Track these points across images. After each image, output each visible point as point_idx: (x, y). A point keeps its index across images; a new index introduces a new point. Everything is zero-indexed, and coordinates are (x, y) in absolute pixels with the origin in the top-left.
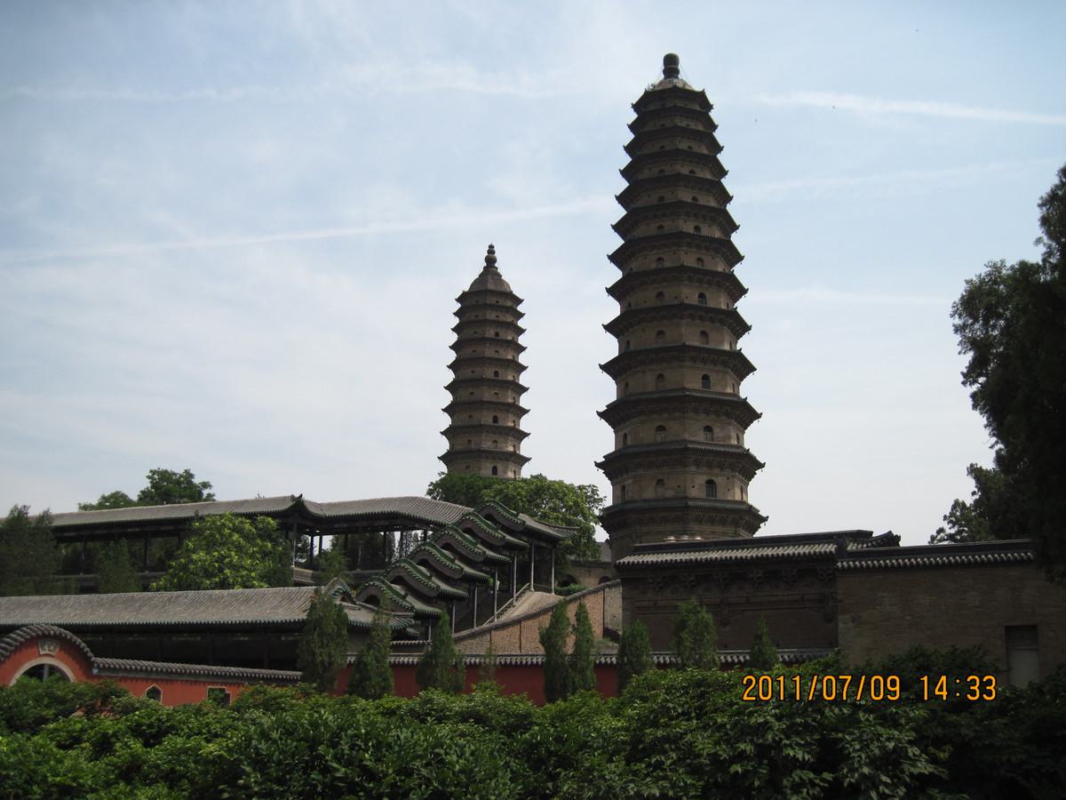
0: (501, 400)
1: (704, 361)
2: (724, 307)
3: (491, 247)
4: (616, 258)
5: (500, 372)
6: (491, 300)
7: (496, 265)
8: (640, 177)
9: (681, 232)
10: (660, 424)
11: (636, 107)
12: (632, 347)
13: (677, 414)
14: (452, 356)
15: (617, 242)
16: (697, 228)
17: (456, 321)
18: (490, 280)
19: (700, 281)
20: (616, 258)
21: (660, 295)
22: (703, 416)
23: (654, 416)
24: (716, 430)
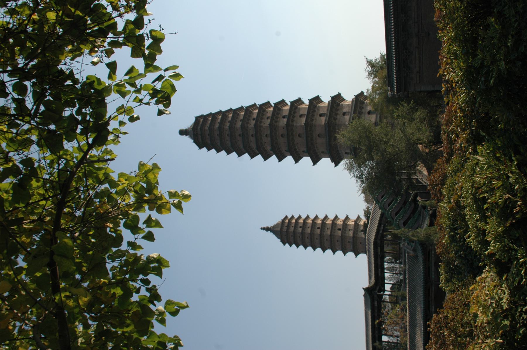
0: (330, 227)
1: (313, 116)
4: (266, 158)
6: (285, 229)
9: (255, 125)
11: (200, 147)
12: (305, 150)
13: (337, 128)
14: (310, 248)
15: (259, 157)
16: (254, 119)
17: (294, 246)
18: (276, 229)
19: (277, 118)
21: (282, 136)
22: (338, 117)
24: (345, 110)
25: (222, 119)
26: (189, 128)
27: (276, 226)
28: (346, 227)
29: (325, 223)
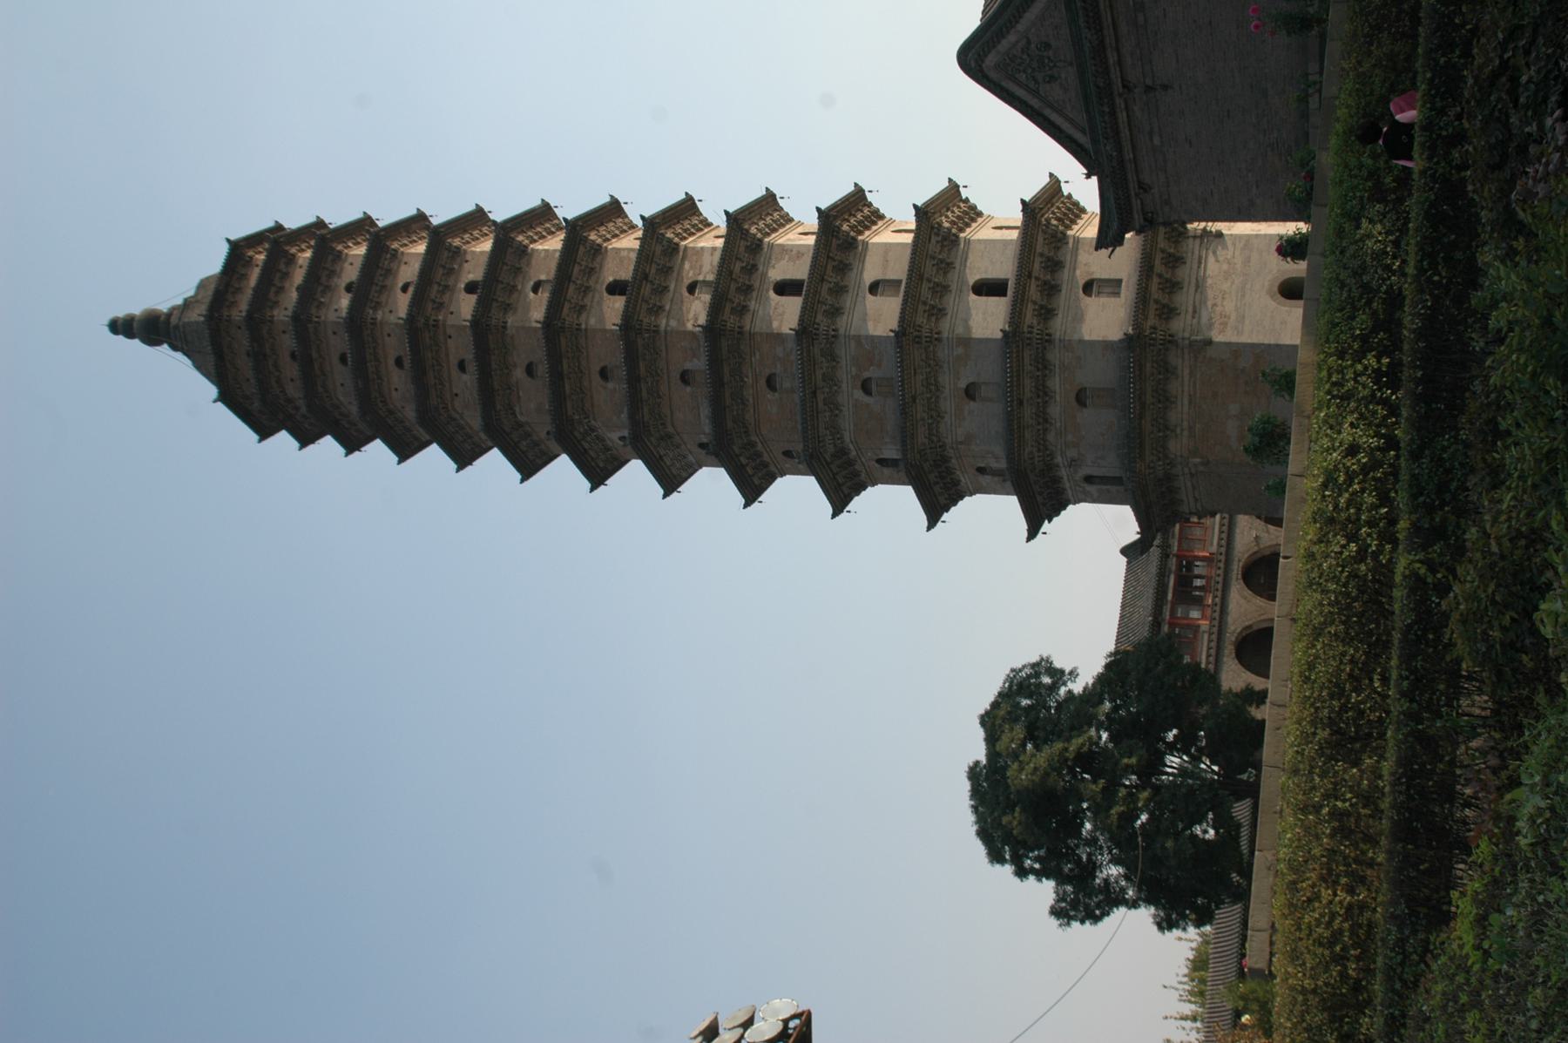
2: (720, 243)
4: (597, 474)
8: (410, 413)
20: (597, 474)
25: (315, 263)
26: (187, 304)
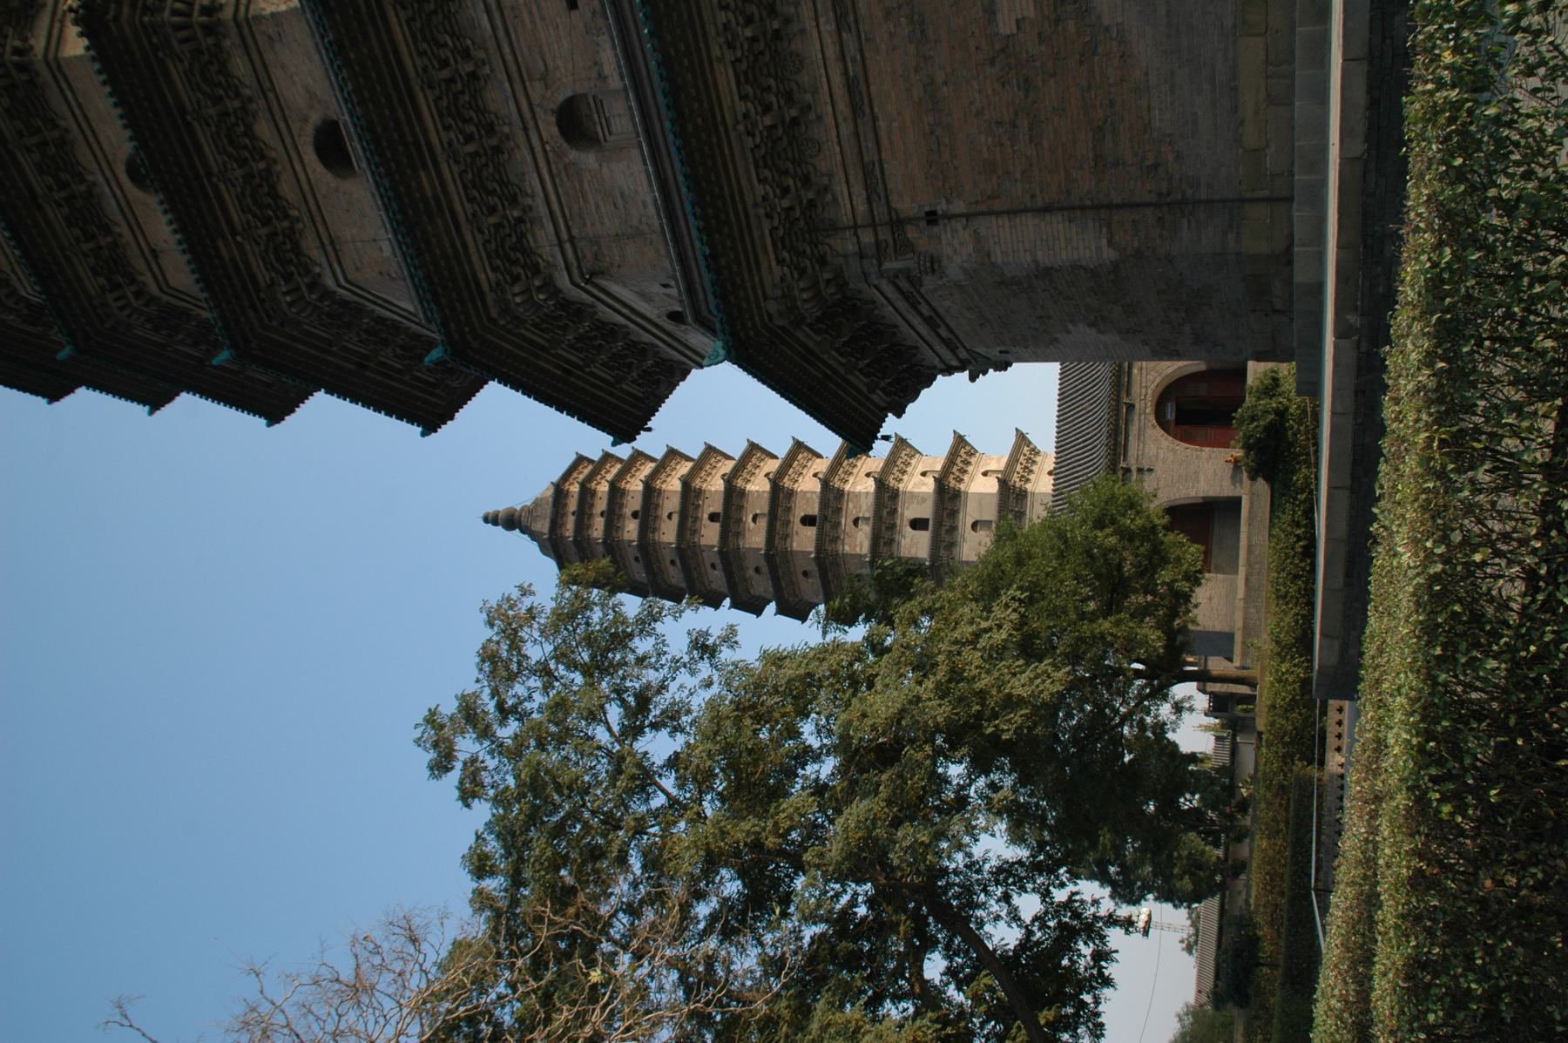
0: (766, 511)
3: (486, 520)
5: (711, 510)
7: (518, 508)
10: (310, 156)
23: (286, 188)
27: (533, 510)
28: (838, 511)
29: (742, 493)
